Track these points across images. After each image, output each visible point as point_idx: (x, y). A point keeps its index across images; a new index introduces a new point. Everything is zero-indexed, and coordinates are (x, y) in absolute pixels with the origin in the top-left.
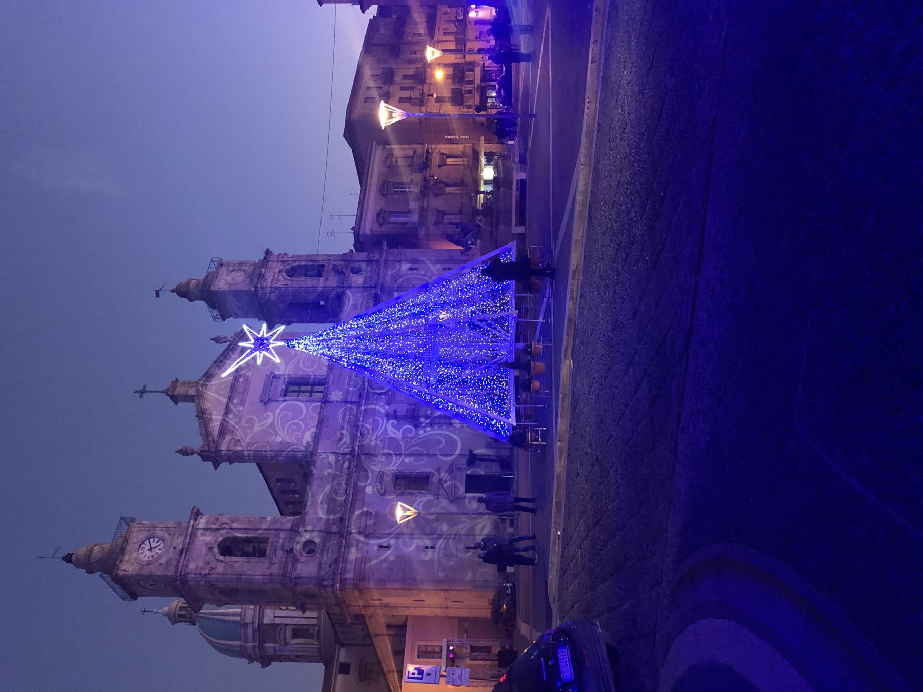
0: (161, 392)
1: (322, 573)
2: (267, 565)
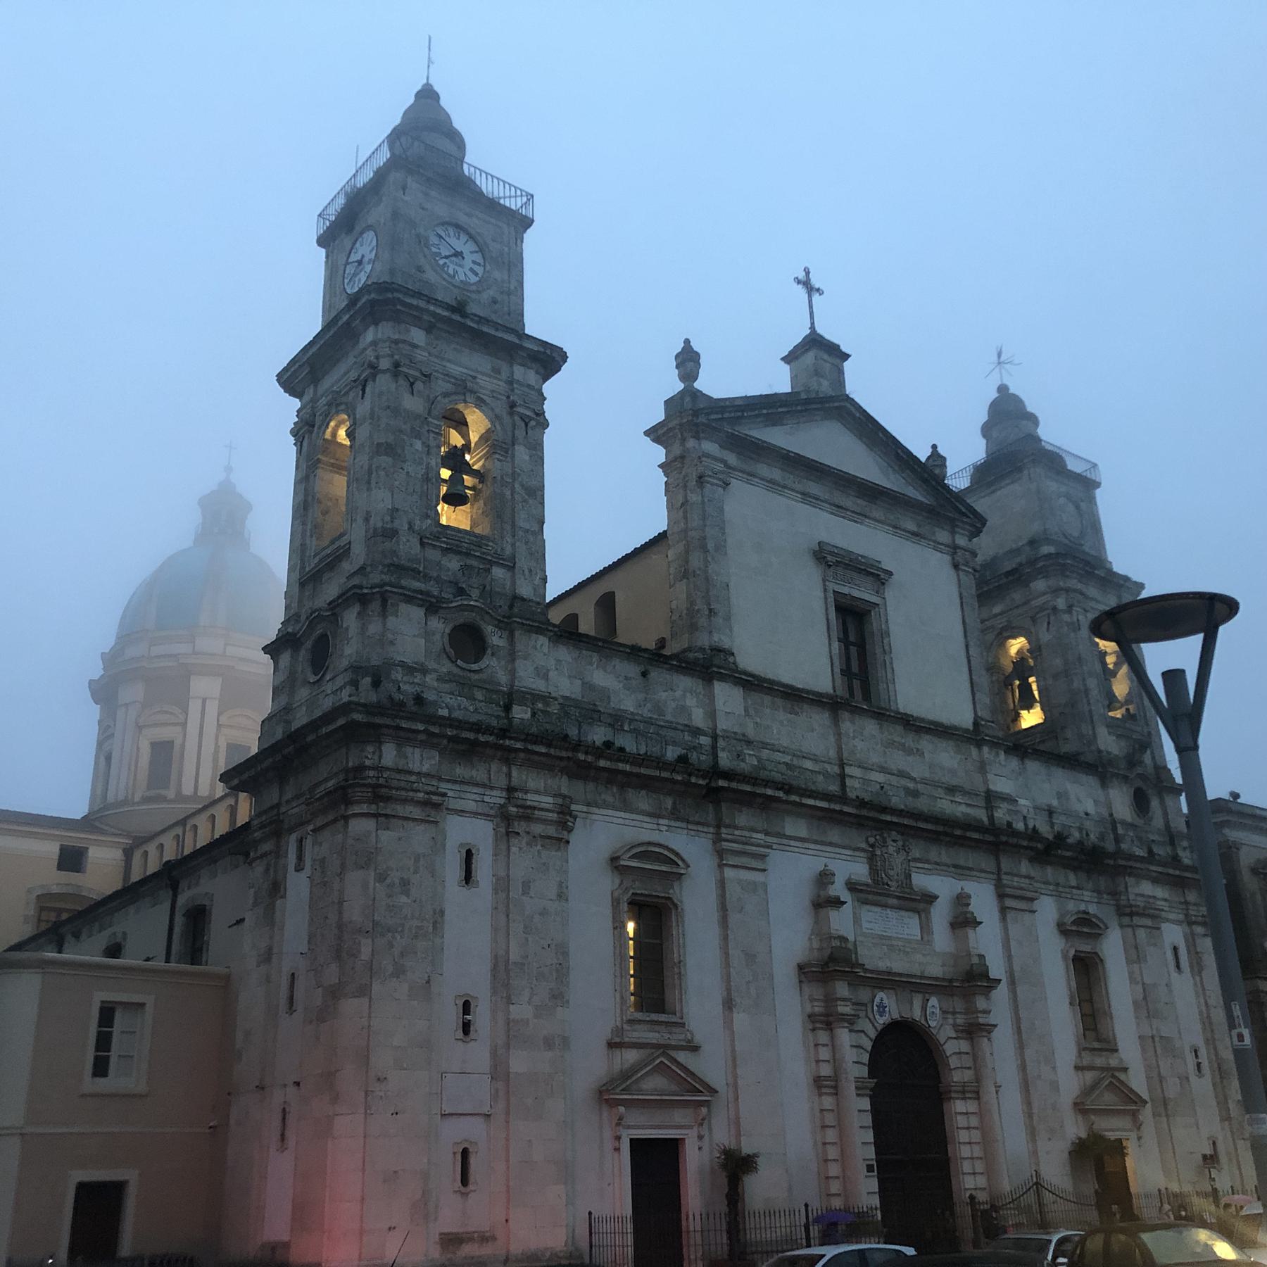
0: (813, 324)
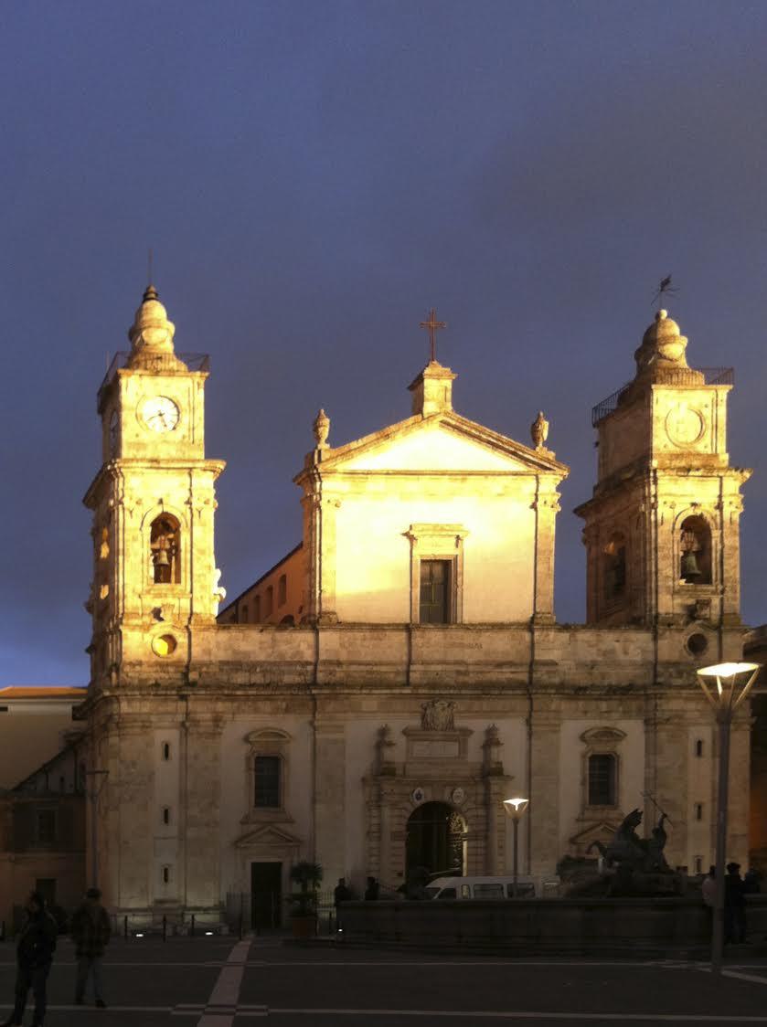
1: (127, 669)
2: (139, 588)
